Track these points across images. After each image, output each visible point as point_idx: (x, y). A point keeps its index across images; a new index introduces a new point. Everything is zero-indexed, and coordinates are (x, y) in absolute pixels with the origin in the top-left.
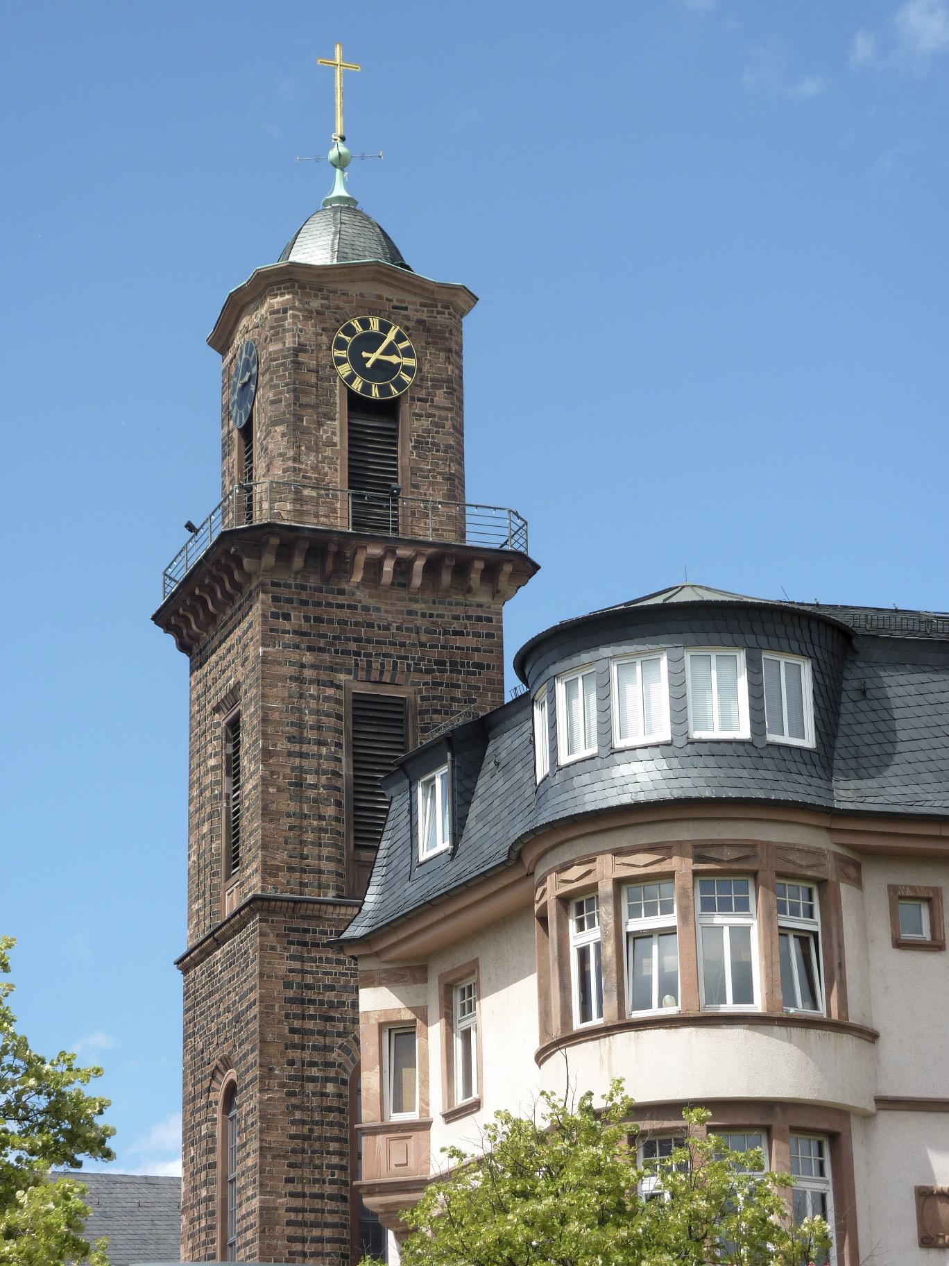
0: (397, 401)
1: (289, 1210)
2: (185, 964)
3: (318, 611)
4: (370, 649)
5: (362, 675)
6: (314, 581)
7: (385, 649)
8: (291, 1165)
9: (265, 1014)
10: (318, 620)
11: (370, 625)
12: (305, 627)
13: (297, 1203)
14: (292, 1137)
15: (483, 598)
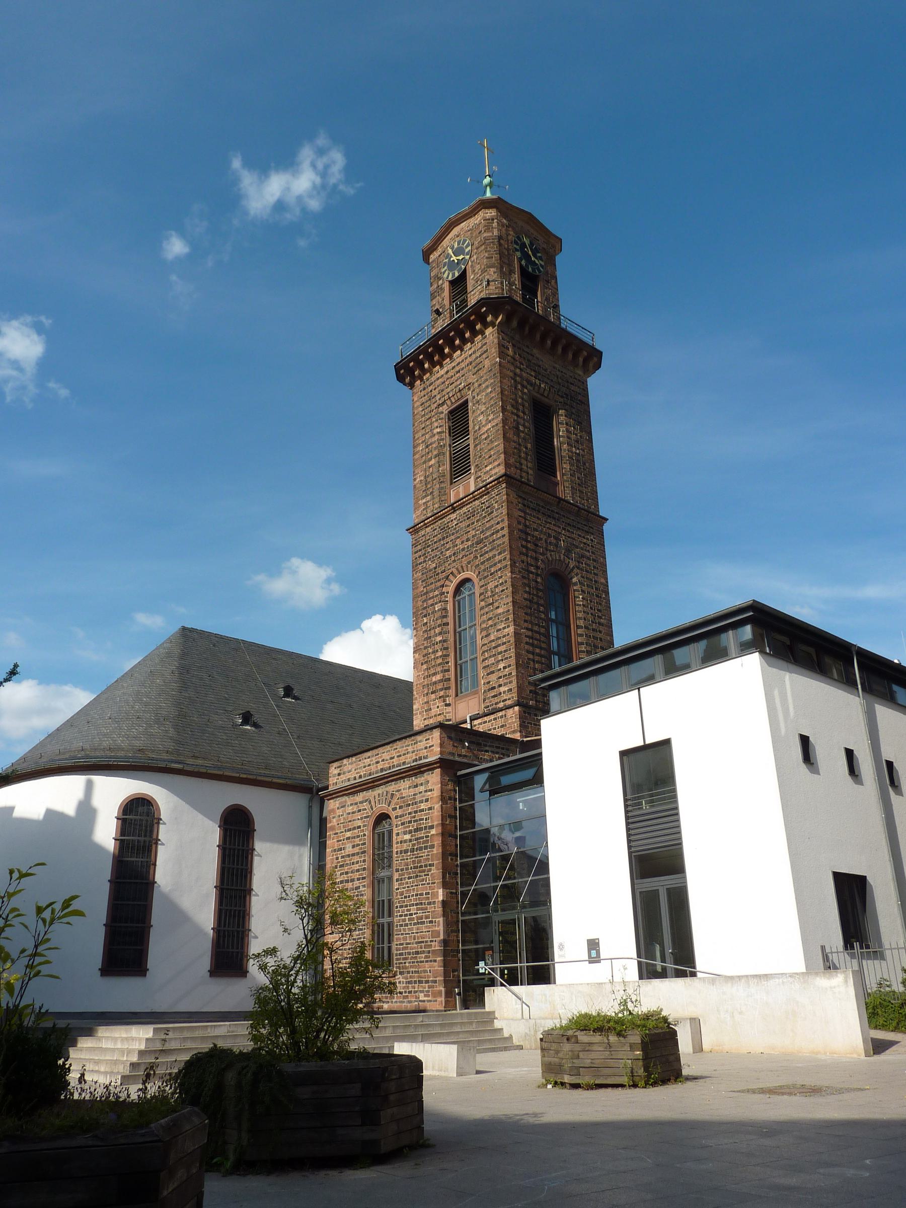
0: (538, 276)
1: (526, 636)
2: (414, 530)
6: (517, 337)
9: (511, 533)
11: (539, 366)
13: (530, 633)
14: (525, 599)
15: (580, 373)
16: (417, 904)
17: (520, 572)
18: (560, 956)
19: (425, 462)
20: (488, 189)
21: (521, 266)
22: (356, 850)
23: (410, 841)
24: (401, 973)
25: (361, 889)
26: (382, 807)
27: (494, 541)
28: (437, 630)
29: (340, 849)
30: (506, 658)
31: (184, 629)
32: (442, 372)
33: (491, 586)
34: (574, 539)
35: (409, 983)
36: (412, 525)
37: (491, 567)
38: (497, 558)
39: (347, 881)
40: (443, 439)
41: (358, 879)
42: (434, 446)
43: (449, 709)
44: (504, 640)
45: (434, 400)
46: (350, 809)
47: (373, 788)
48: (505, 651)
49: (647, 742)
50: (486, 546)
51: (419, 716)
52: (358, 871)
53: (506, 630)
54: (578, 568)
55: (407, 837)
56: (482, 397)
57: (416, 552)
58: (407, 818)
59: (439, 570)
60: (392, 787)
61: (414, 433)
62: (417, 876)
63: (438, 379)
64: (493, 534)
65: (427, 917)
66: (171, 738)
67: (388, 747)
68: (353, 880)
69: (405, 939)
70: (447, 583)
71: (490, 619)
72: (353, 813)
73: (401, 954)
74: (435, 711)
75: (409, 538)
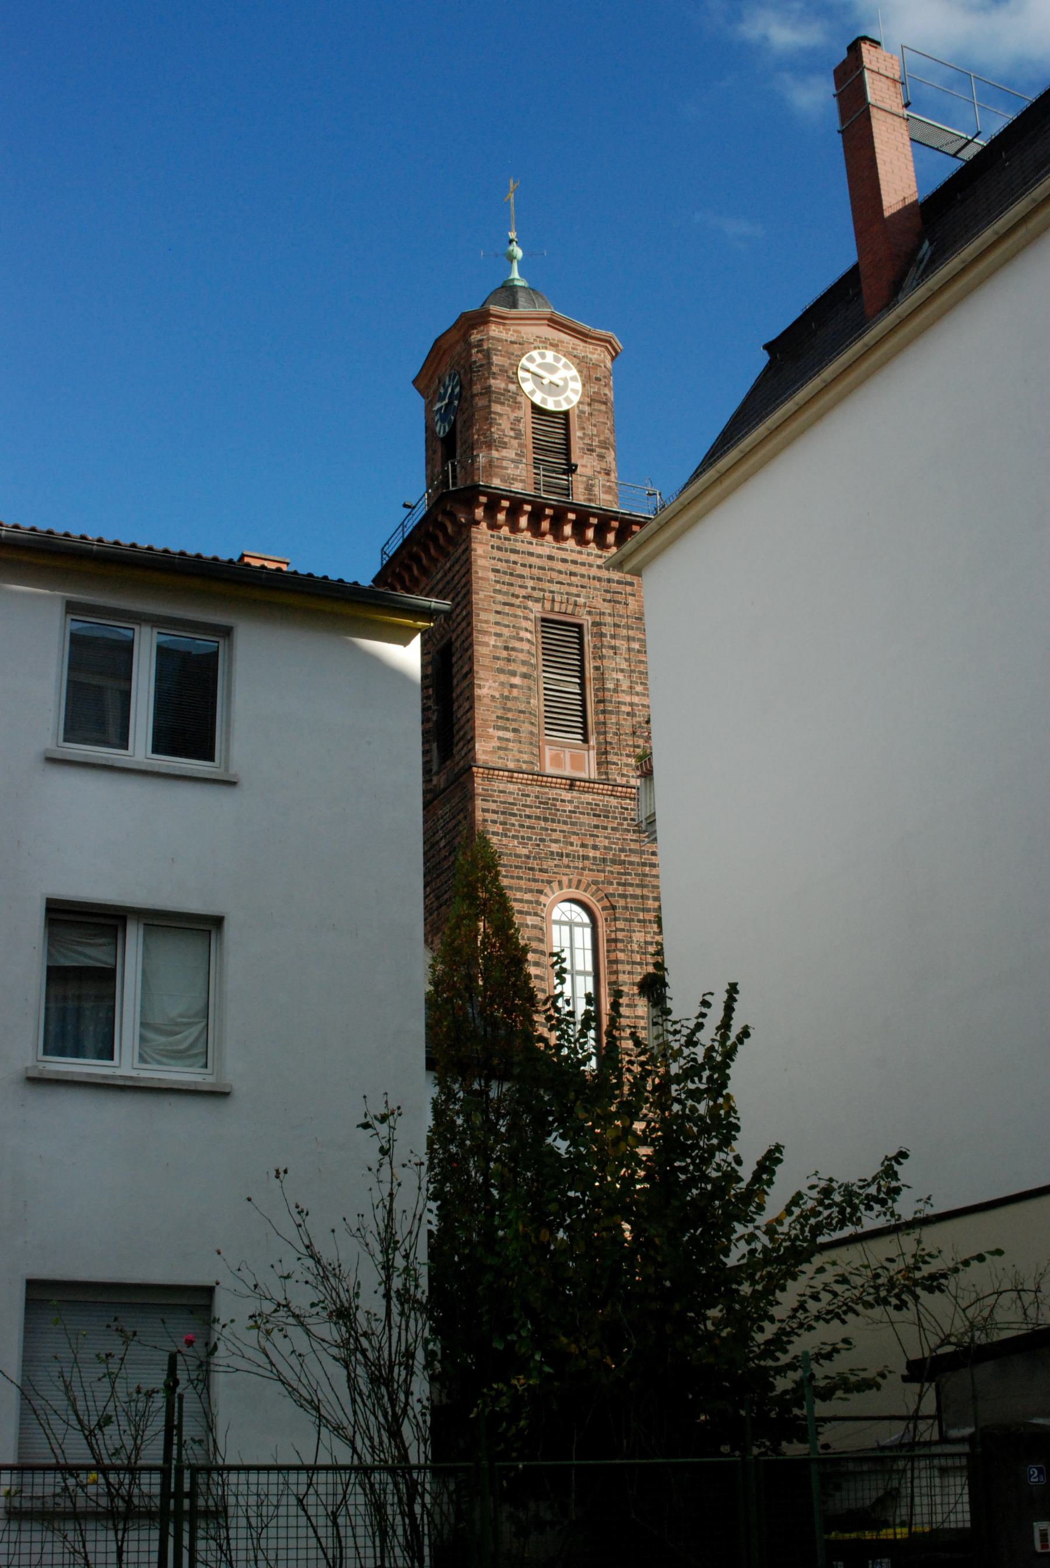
19: (501, 671)
64: (644, 864)
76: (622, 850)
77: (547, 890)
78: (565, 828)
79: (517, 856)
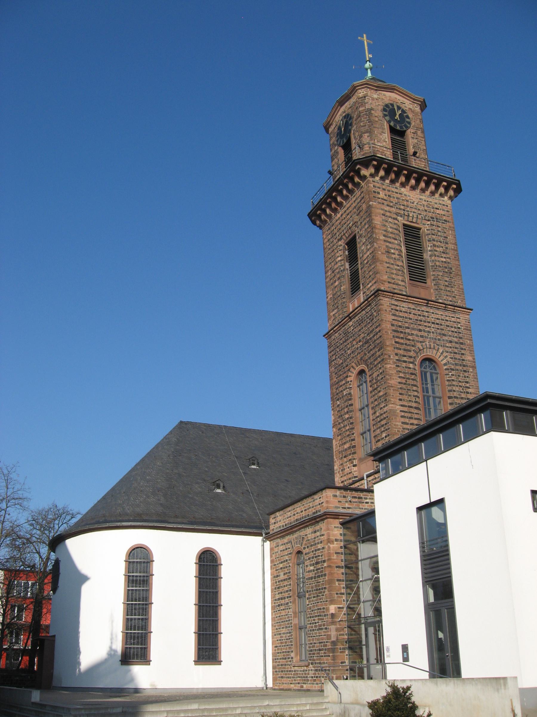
1: (401, 411)
2: (328, 335)
3: (390, 193)
4: (408, 209)
5: (406, 217)
7: (413, 210)
8: (400, 394)
10: (389, 196)
11: (407, 201)
12: (385, 198)
14: (399, 383)
16: (318, 616)
17: (395, 363)
18: (388, 656)
20: (369, 71)
21: (390, 127)
22: (286, 577)
23: (314, 571)
24: (312, 663)
25: (290, 604)
26: (297, 547)
27: (375, 341)
28: (346, 410)
29: (277, 576)
30: (386, 430)
31: (181, 422)
32: (339, 215)
33: (375, 375)
34: (443, 330)
35: (316, 670)
36: (327, 331)
37: (375, 360)
38: (378, 354)
39: (282, 599)
40: (342, 266)
41: (288, 597)
42: (337, 271)
43: (355, 469)
44: (385, 416)
45: (335, 237)
46: (281, 548)
47: (292, 533)
48: (386, 424)
49: (432, 501)
50: (371, 345)
51: (338, 474)
52: (287, 591)
53: (386, 408)
54: (447, 352)
55: (312, 568)
56: (363, 232)
57: (331, 352)
58: (311, 555)
59: (344, 365)
60: (302, 533)
61: (325, 262)
62: (318, 596)
63: (337, 221)
65: (324, 625)
66: (161, 504)
67: (299, 504)
68: (284, 598)
69: (313, 640)
70: (350, 374)
71: (376, 400)
72: (283, 550)
73: (311, 651)
74: (347, 470)
75: (325, 342)
76: (368, 335)
77: (350, 374)
78: (351, 340)
79: (340, 365)
